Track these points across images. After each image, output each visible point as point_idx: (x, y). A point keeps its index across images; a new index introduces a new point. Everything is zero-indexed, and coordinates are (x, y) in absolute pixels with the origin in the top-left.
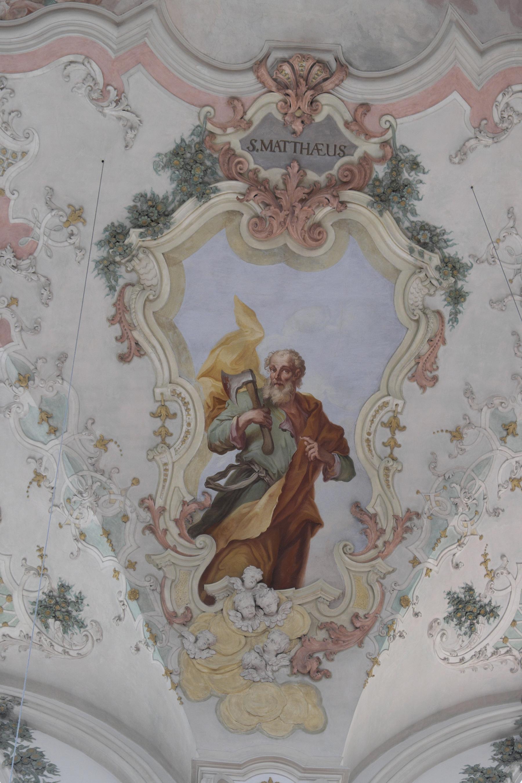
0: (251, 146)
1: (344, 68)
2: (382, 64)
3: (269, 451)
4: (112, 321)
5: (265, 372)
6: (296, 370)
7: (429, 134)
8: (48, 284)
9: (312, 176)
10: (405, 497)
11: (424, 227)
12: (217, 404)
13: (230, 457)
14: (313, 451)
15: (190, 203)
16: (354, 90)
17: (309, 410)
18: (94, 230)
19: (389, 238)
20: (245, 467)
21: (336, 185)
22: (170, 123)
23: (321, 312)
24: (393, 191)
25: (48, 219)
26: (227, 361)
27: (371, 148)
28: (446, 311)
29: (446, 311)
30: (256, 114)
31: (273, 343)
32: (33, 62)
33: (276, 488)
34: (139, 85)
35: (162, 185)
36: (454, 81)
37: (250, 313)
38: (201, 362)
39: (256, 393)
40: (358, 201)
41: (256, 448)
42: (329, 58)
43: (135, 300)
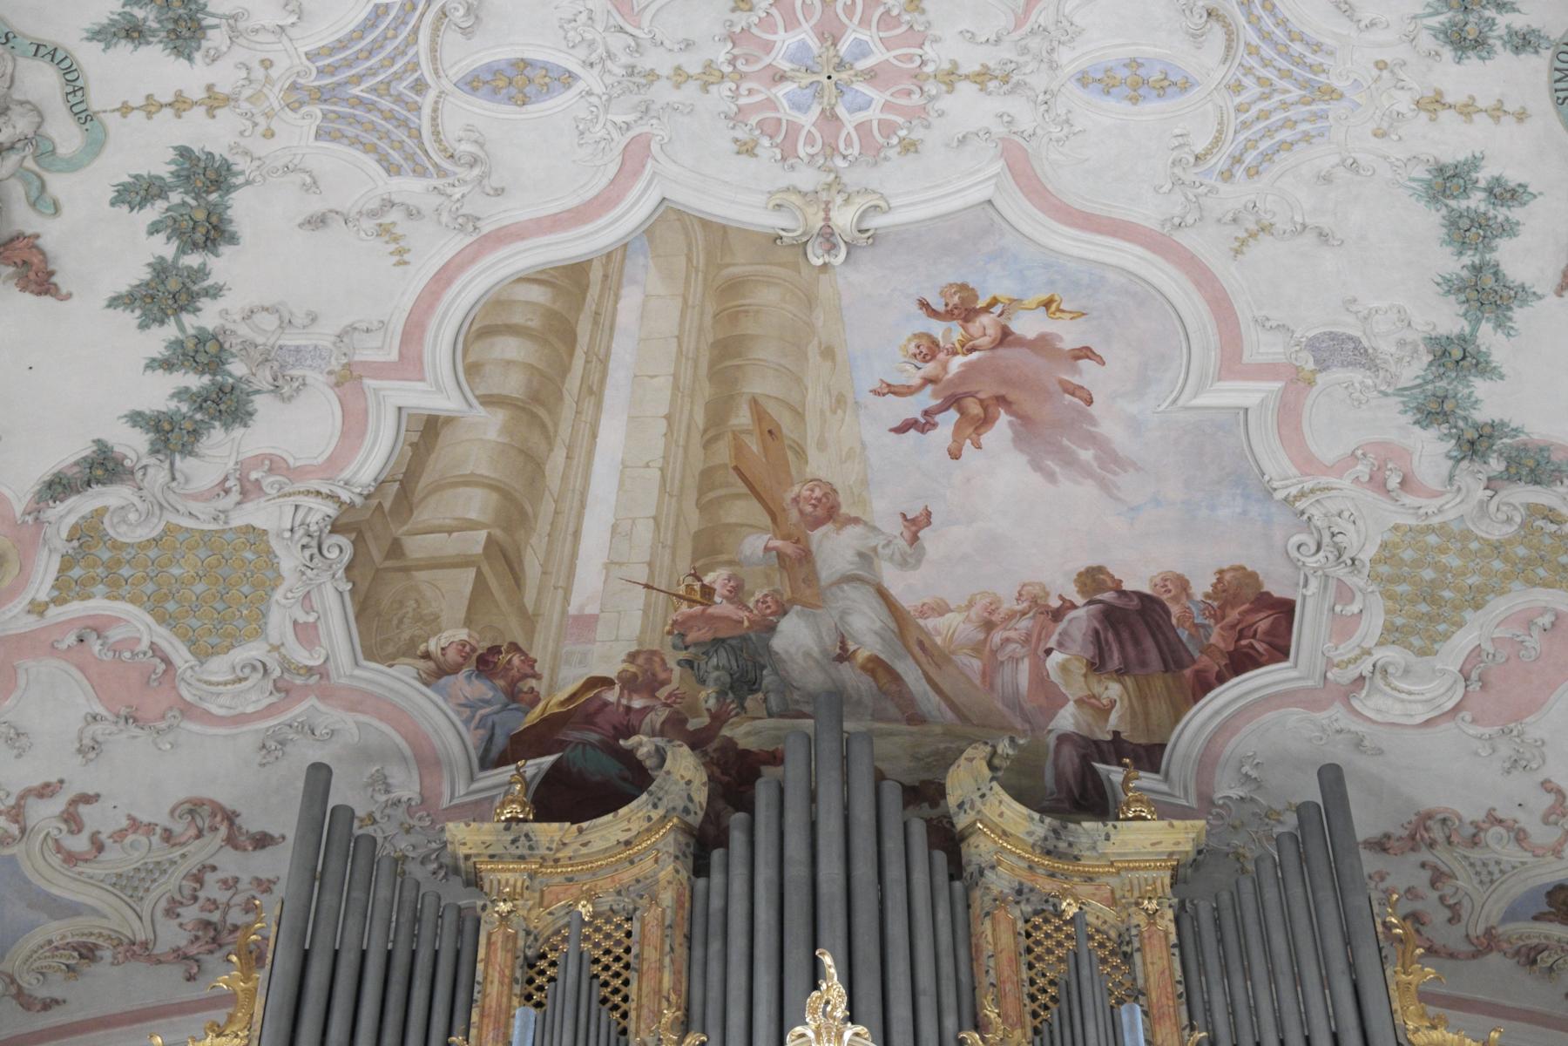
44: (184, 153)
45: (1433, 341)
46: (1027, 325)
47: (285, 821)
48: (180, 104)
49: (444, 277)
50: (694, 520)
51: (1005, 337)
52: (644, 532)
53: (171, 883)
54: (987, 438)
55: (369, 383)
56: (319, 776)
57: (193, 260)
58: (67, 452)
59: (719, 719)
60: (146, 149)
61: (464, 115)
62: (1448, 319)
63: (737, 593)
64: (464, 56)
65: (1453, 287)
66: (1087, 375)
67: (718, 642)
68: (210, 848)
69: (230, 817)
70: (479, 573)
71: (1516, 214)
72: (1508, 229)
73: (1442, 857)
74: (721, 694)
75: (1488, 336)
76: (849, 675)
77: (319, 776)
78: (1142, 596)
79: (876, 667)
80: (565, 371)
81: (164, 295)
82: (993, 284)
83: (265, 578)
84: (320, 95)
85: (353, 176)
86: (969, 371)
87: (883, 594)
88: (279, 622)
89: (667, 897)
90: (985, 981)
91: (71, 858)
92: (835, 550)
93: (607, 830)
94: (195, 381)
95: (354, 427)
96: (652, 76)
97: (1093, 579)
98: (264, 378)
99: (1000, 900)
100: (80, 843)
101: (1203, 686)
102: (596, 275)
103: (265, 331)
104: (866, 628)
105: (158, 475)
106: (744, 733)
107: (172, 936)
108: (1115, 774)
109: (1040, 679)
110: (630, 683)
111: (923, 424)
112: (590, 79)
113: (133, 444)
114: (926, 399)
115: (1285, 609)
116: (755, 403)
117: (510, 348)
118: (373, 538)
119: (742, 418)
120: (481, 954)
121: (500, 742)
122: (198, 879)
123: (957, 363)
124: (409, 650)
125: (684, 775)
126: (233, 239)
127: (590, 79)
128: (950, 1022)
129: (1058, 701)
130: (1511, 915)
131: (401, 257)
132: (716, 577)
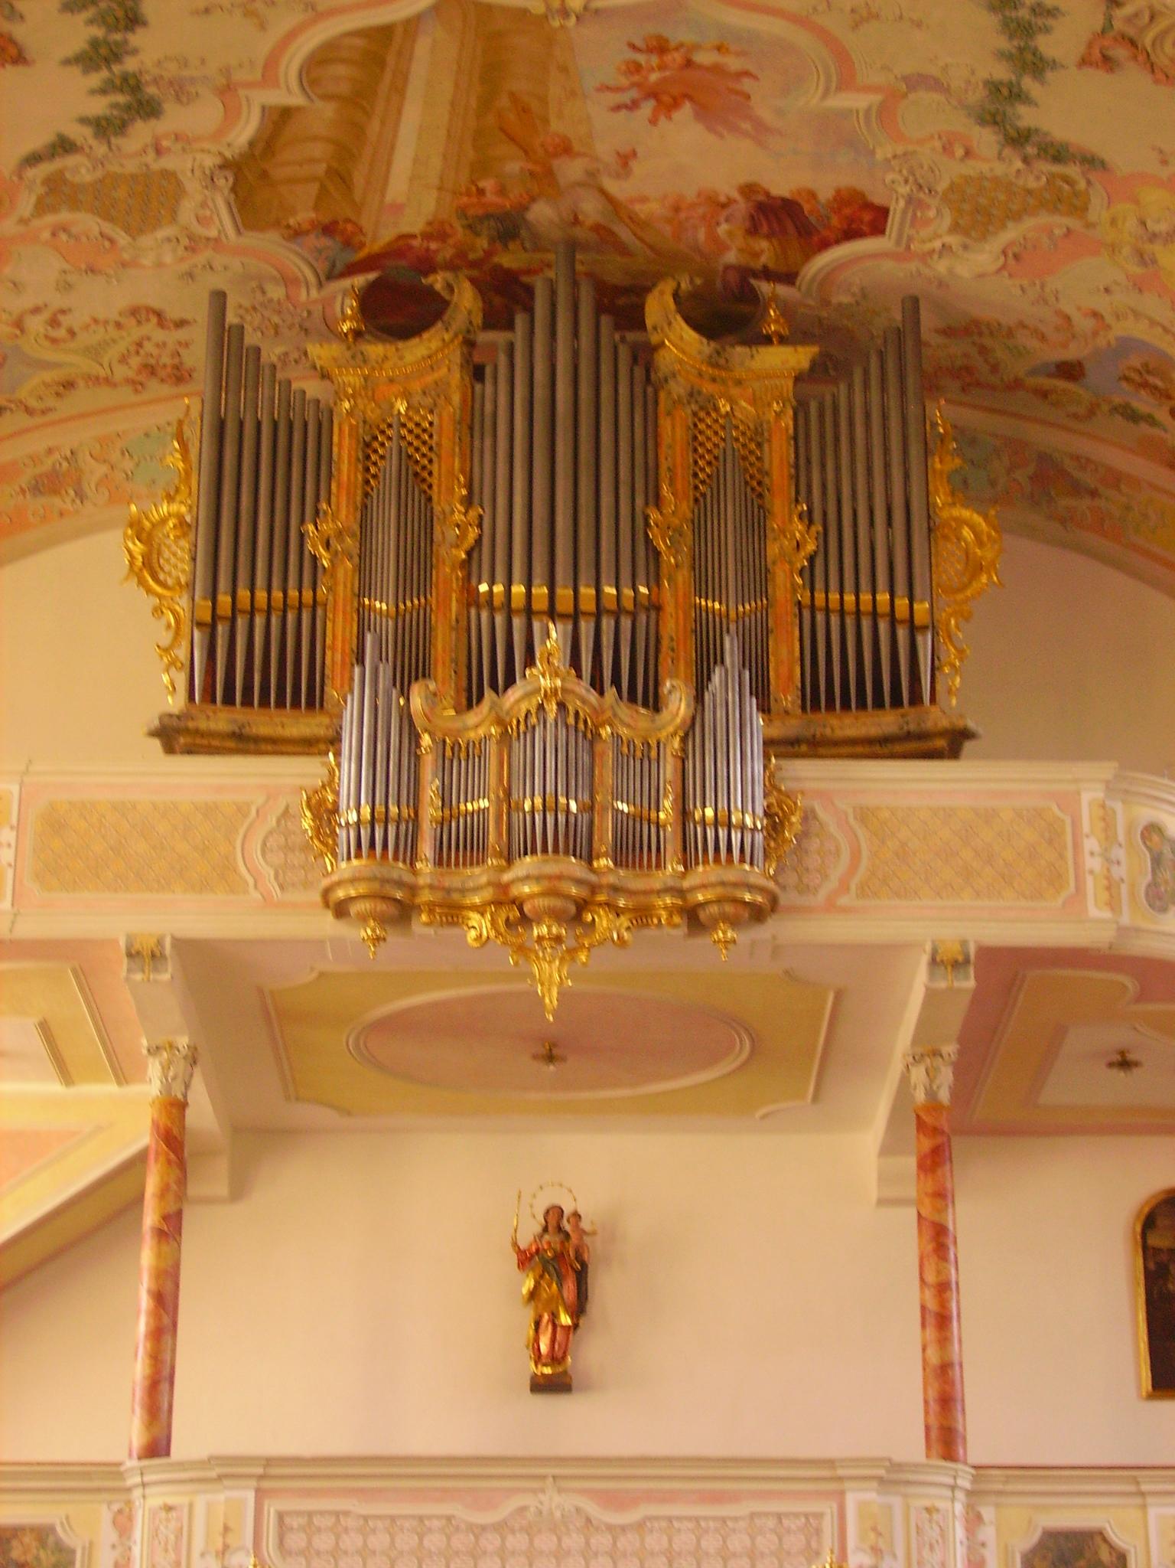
45: (988, 83)
46: (703, 58)
47: (200, 314)
49: (292, 35)
50: (471, 154)
51: (689, 63)
52: (436, 163)
53: (121, 347)
54: (677, 115)
55: (242, 92)
56: (219, 298)
57: (118, 37)
59: (489, 254)
62: (1002, 72)
63: (502, 191)
65: (1002, 56)
66: (747, 85)
67: (488, 216)
68: (150, 328)
69: (159, 315)
70: (323, 187)
71: (1050, 22)
72: (1047, 30)
73: (987, 341)
74: (492, 241)
75: (1028, 83)
76: (580, 233)
77: (219, 298)
78: (783, 200)
79: (597, 228)
81: (98, 56)
82: (679, 35)
83: (179, 192)
86: (664, 80)
87: (603, 192)
88: (187, 210)
89: (456, 398)
90: (664, 465)
91: (54, 341)
92: (570, 170)
93: (416, 350)
94: (121, 99)
97: (748, 190)
99: (677, 403)
100: (61, 333)
101: (825, 245)
102: (399, 31)
103: (171, 70)
104: (591, 208)
105: (101, 149)
106: (508, 260)
107: (121, 372)
108: (765, 288)
109: (712, 236)
110: (427, 236)
111: (633, 106)
113: (81, 134)
114: (633, 94)
115: (883, 212)
116: (512, 96)
118: (250, 180)
119: (504, 102)
120: (336, 439)
121: (339, 266)
122: (140, 345)
123: (654, 77)
124: (277, 224)
125: (466, 301)
126: (145, 24)
128: (640, 501)
129: (723, 248)
130: (1033, 372)
131: (262, 26)
132: (488, 184)
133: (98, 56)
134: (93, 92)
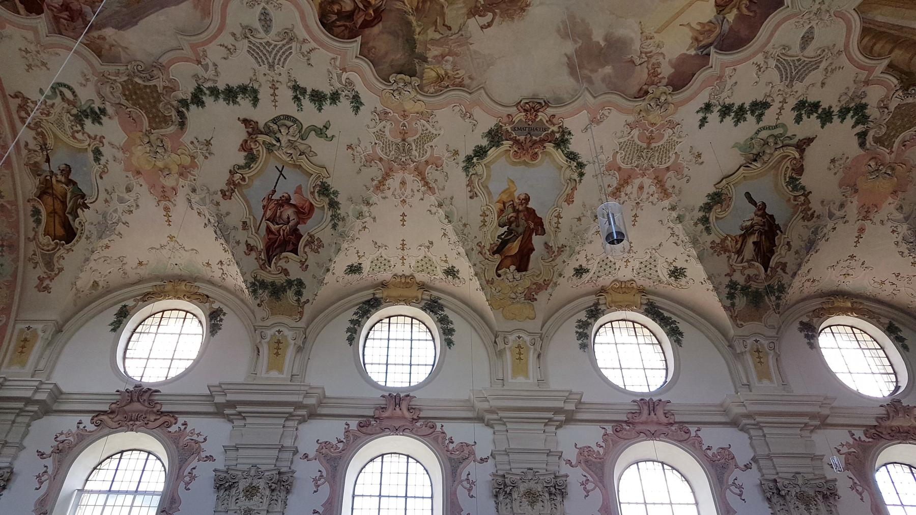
0: (514, 129)
1: (547, 104)
2: (560, 102)
3: (518, 226)
4: (468, 185)
5: (517, 201)
6: (527, 199)
7: (575, 123)
8: (447, 175)
9: (534, 138)
10: (562, 241)
11: (572, 153)
12: (501, 211)
13: (505, 228)
14: (532, 226)
15: (493, 148)
16: (550, 111)
17: (531, 213)
18: (462, 157)
19: (559, 157)
20: (510, 232)
21: (542, 141)
22: (488, 123)
23: (536, 180)
24: (561, 142)
25: (447, 154)
26: (505, 197)
27: (555, 129)
28: (577, 180)
29: (577, 180)
30: (516, 119)
31: (519, 192)
32: (441, 107)
33: (520, 238)
34: (477, 112)
35: (485, 142)
36: (584, 107)
37: (513, 182)
38: (496, 198)
39: (514, 207)
40: (550, 147)
41: (513, 225)
42: (542, 101)
43: (475, 179)
44: (793, 109)
48: (781, 108)
49: (851, 59)
57: (820, 111)
58: (855, 141)
60: (789, 116)
61: (810, 51)
64: (796, 50)
80: (892, 34)
84: (791, 81)
85: (816, 76)
94: (851, 113)
95: (879, 82)
96: (819, 9)
98: (857, 101)
102: (867, 25)
103: (845, 99)
112: (813, 23)
113: (860, 128)
117: (877, 47)
127: (813, 23)
133: (826, 117)
134: (842, 122)
